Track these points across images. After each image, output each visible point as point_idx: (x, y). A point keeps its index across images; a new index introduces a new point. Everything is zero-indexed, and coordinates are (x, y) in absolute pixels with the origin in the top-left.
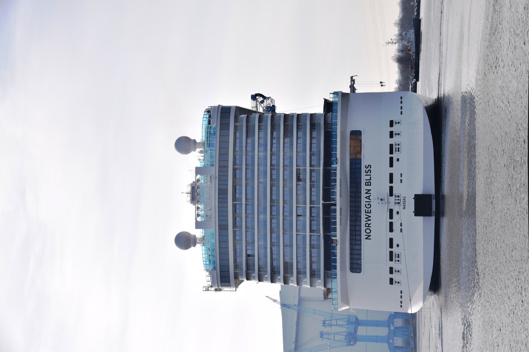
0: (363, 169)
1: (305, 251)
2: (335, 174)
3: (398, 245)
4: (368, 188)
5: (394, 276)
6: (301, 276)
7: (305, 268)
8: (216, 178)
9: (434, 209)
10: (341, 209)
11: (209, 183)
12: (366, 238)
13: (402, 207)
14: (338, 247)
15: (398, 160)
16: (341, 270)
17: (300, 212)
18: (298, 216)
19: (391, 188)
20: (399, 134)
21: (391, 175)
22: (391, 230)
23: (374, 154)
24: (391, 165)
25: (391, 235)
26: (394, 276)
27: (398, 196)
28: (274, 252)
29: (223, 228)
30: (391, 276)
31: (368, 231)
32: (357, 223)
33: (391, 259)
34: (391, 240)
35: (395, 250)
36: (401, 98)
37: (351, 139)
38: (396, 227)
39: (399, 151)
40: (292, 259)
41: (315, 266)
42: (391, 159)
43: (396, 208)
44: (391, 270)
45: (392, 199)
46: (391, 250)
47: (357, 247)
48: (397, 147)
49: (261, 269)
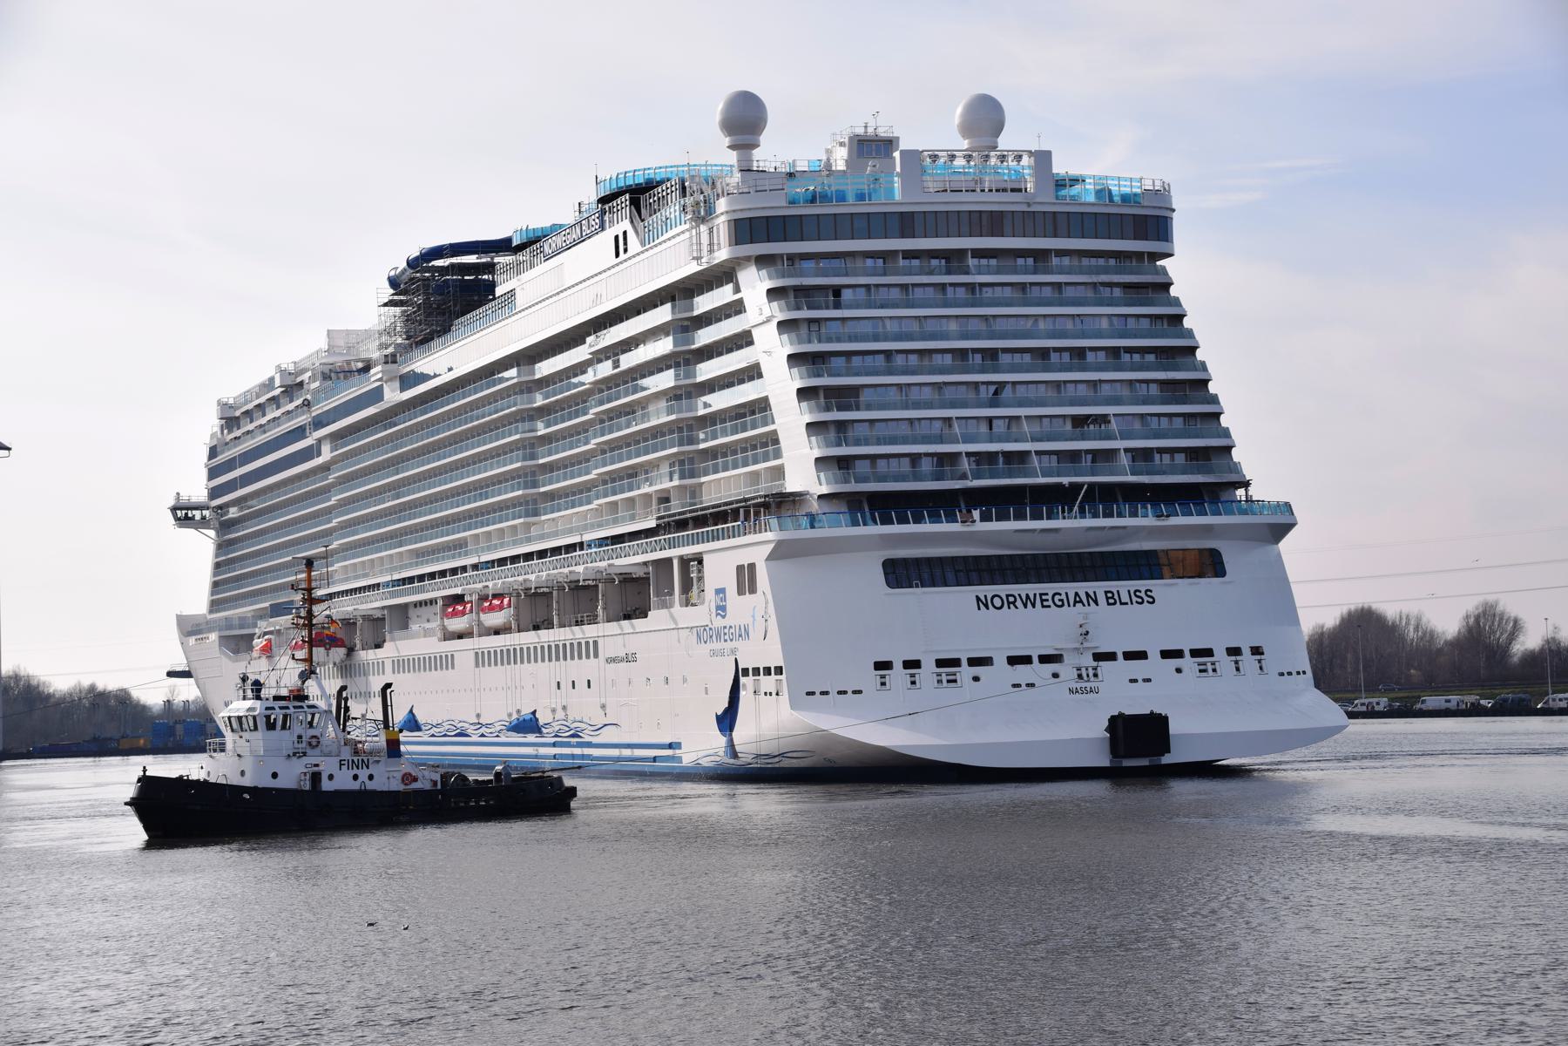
0: (1142, 585)
1: (905, 441)
3: (976, 679)
4: (1101, 598)
5: (898, 675)
6: (832, 435)
7: (857, 443)
8: (1029, 205)
9: (1127, 763)
10: (1056, 530)
11: (940, 186)
12: (978, 599)
13: (1074, 685)
14: (945, 527)
15: (1179, 671)
16: (881, 536)
17: (999, 427)
18: (990, 420)
19: (1111, 656)
20: (1238, 669)
22: (1013, 661)
23: (1179, 609)
24: (1166, 654)
26: (898, 675)
27: (1096, 675)
28: (869, 359)
29: (906, 223)
30: (898, 665)
31: (997, 602)
32: (974, 575)
33: (941, 663)
35: (965, 672)
37: (1201, 551)
38: (1022, 673)
40: (869, 407)
41: (862, 467)
42: (1178, 654)
43: (1066, 670)
46: (964, 662)
47: (950, 576)
48: (1210, 667)
49: (814, 327)
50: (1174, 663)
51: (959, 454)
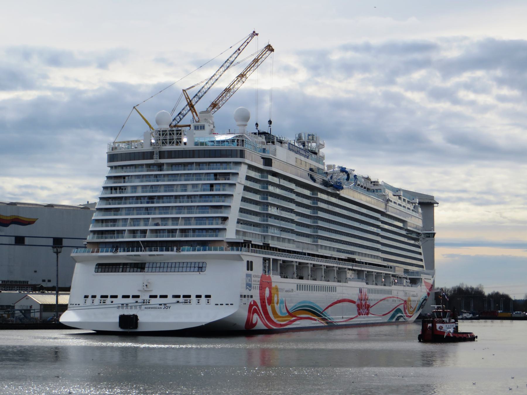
2: (167, 250)
3: (112, 302)
5: (90, 299)
10: (139, 255)
15: (178, 302)
19: (155, 297)
21: (166, 297)
22: (124, 297)
25: (120, 297)
26: (90, 299)
30: (90, 297)
33: (102, 297)
34: (116, 297)
35: (109, 300)
36: (232, 304)
38: (126, 301)
39: (185, 302)
42: (179, 296)
44: (94, 297)
45: (147, 298)
46: (109, 297)
50: (176, 299)
51: (147, 230)
